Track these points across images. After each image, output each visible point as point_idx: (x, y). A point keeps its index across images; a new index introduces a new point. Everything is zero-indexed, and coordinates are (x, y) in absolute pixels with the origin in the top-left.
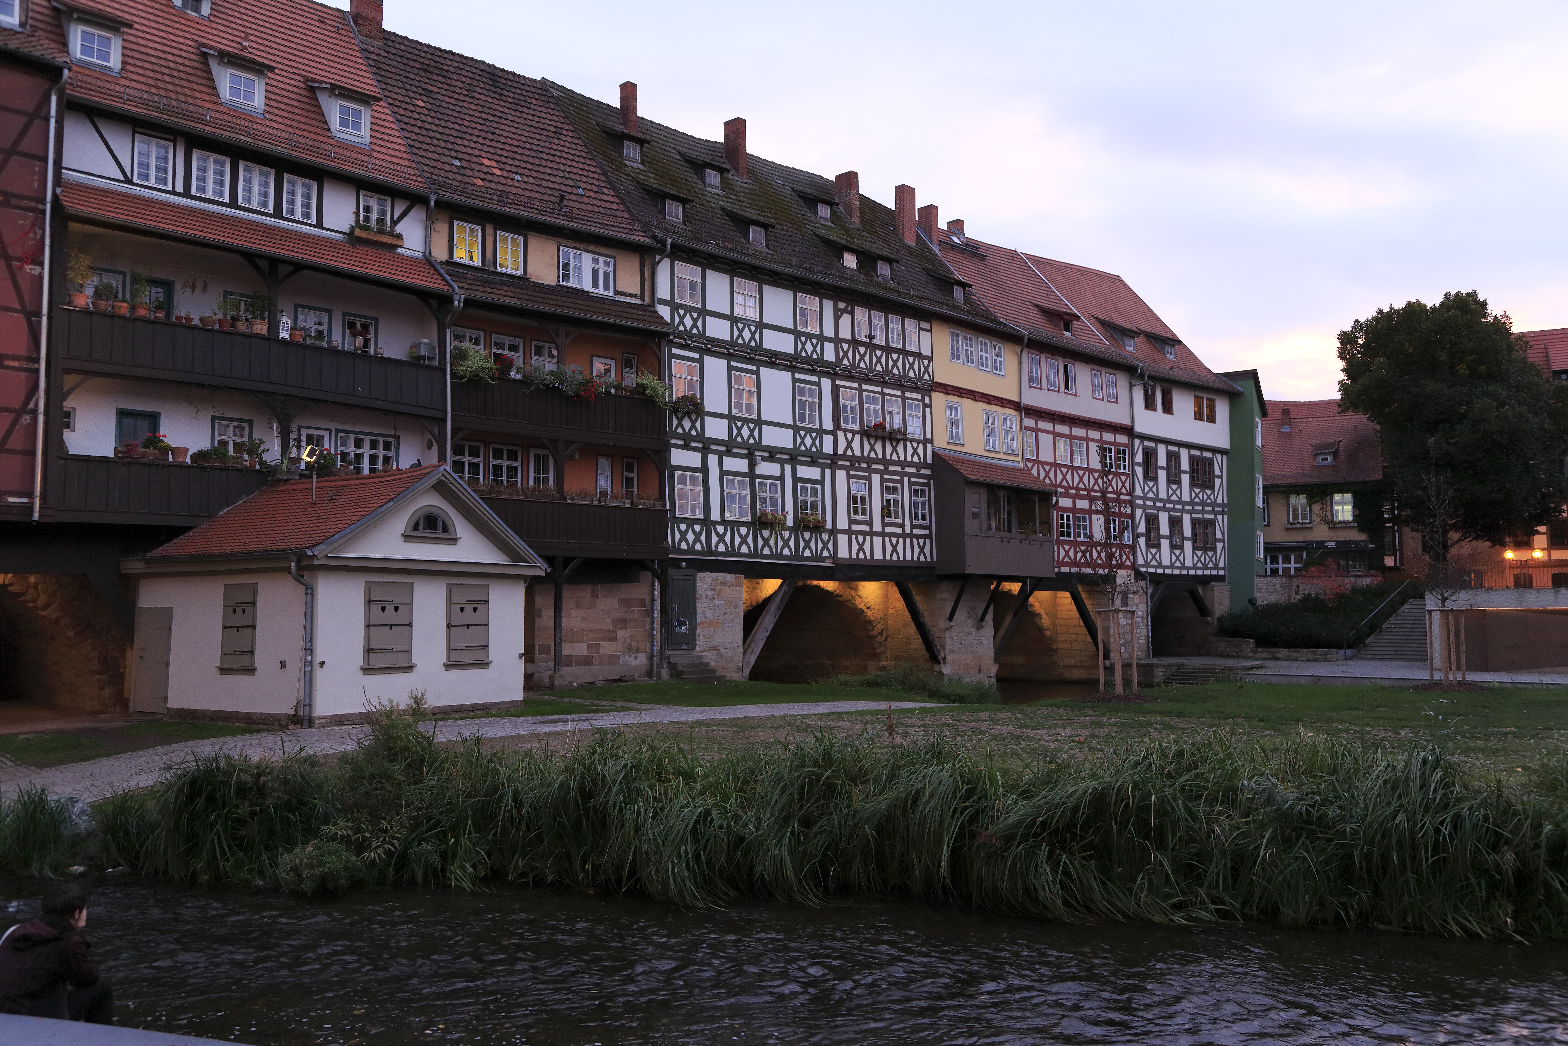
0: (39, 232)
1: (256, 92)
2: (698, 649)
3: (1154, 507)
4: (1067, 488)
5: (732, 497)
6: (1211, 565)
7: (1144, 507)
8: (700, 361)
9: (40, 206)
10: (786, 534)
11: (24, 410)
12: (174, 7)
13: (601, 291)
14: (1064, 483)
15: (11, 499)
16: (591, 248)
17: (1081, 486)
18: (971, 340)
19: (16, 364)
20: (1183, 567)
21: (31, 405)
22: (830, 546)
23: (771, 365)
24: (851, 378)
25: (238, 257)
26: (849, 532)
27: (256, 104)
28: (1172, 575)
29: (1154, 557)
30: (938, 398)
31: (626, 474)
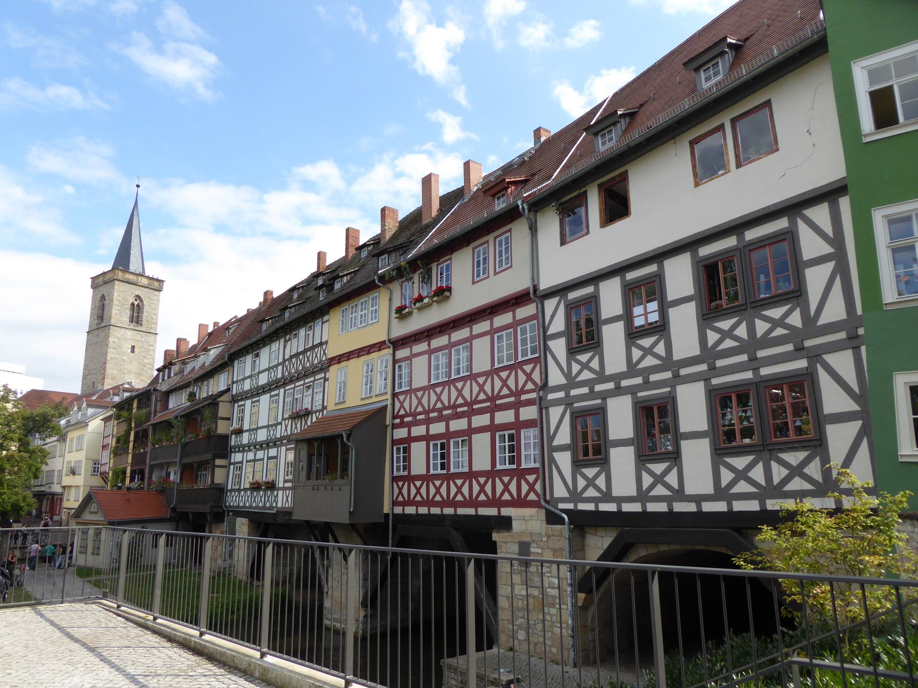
3: (592, 395)
4: (440, 411)
6: (797, 484)
7: (568, 402)
8: (244, 405)
13: (226, 388)
14: (439, 405)
17: (460, 401)
18: (356, 305)
20: (679, 494)
23: (264, 392)
24: (291, 381)
26: (284, 489)
28: (644, 514)
29: (591, 482)
30: (334, 372)
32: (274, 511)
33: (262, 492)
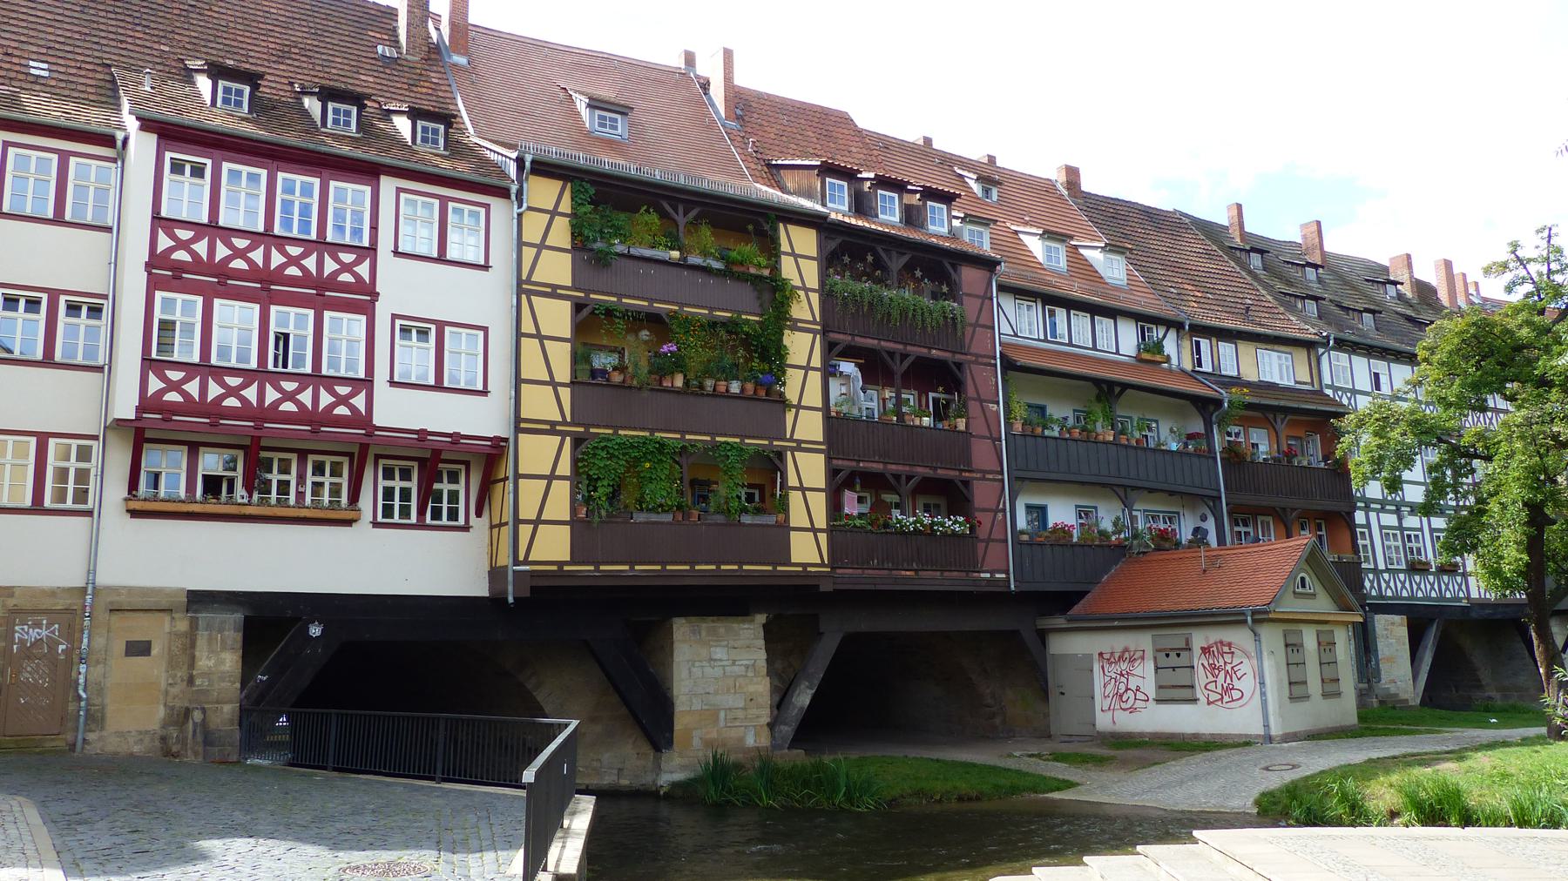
0: (994, 380)
1: (1061, 256)
2: (1383, 681)
5: (1389, 547)
9: (993, 362)
10: (1431, 578)
11: (996, 511)
12: (978, 198)
15: (998, 576)
16: (1276, 347)
19: (991, 476)
21: (1001, 506)
22: (1464, 587)
25: (1089, 384)
27: (1061, 265)
31: (1318, 533)
32: (1464, 603)
33: (1431, 578)
